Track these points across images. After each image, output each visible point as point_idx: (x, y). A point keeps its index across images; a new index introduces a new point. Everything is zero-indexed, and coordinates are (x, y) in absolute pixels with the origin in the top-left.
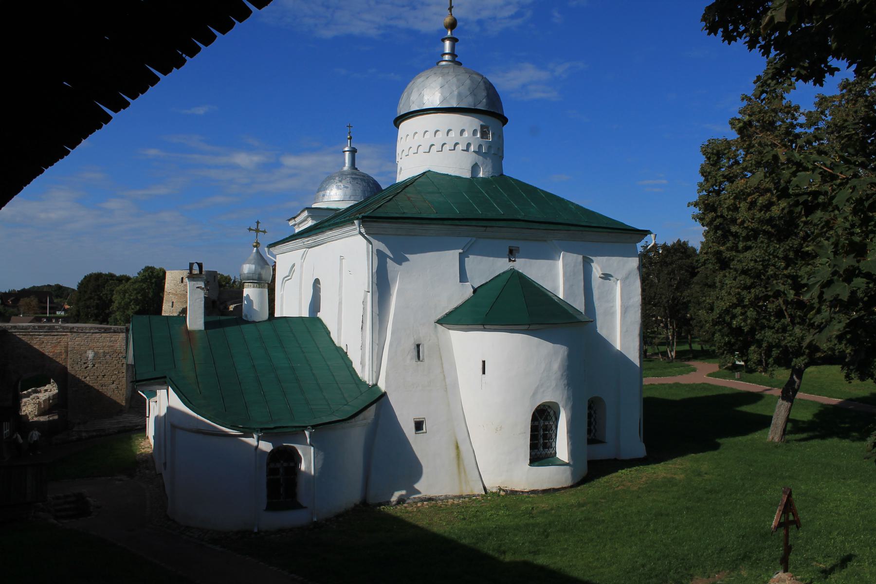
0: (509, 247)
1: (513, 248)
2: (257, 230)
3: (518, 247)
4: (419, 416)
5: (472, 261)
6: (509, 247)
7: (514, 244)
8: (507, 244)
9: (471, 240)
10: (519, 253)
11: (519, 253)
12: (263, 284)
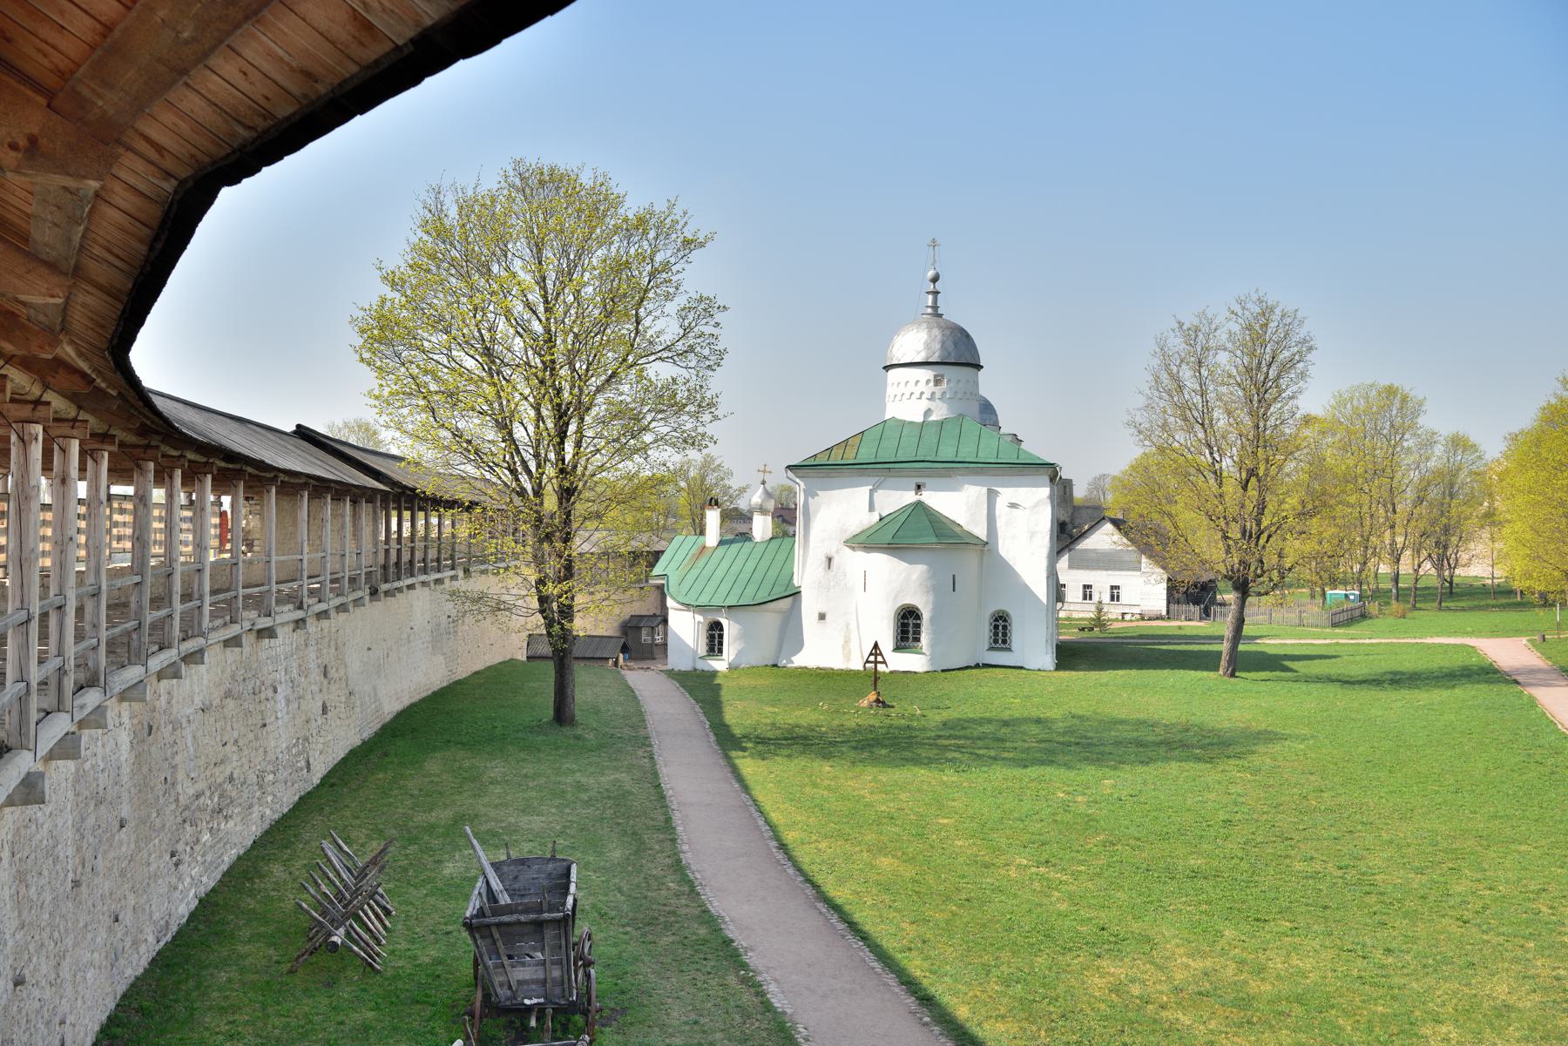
2: (764, 472)
4: (823, 611)
5: (880, 495)
8: (914, 481)
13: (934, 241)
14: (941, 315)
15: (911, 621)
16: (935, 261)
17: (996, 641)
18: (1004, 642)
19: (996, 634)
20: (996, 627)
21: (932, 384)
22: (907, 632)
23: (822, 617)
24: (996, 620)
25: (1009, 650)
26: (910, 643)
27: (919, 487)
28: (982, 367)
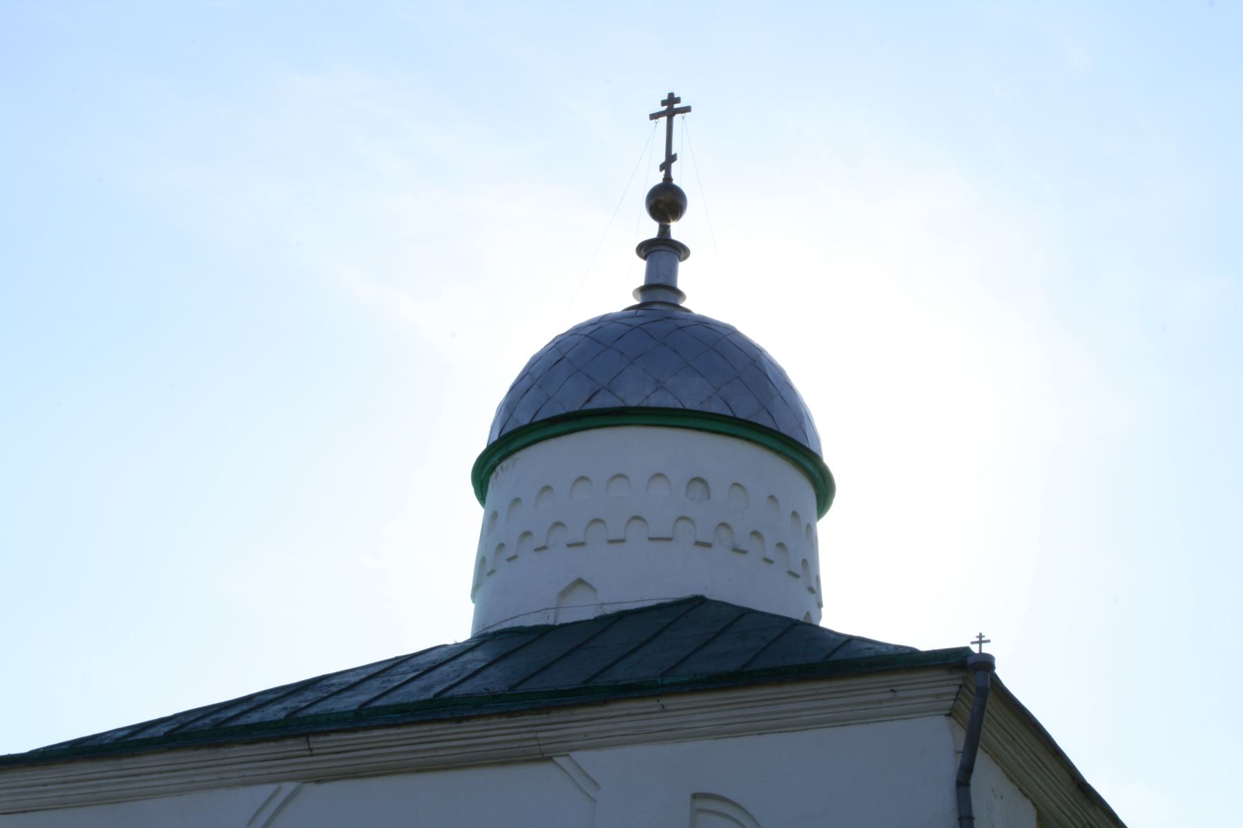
13: (671, 100)
16: (670, 158)
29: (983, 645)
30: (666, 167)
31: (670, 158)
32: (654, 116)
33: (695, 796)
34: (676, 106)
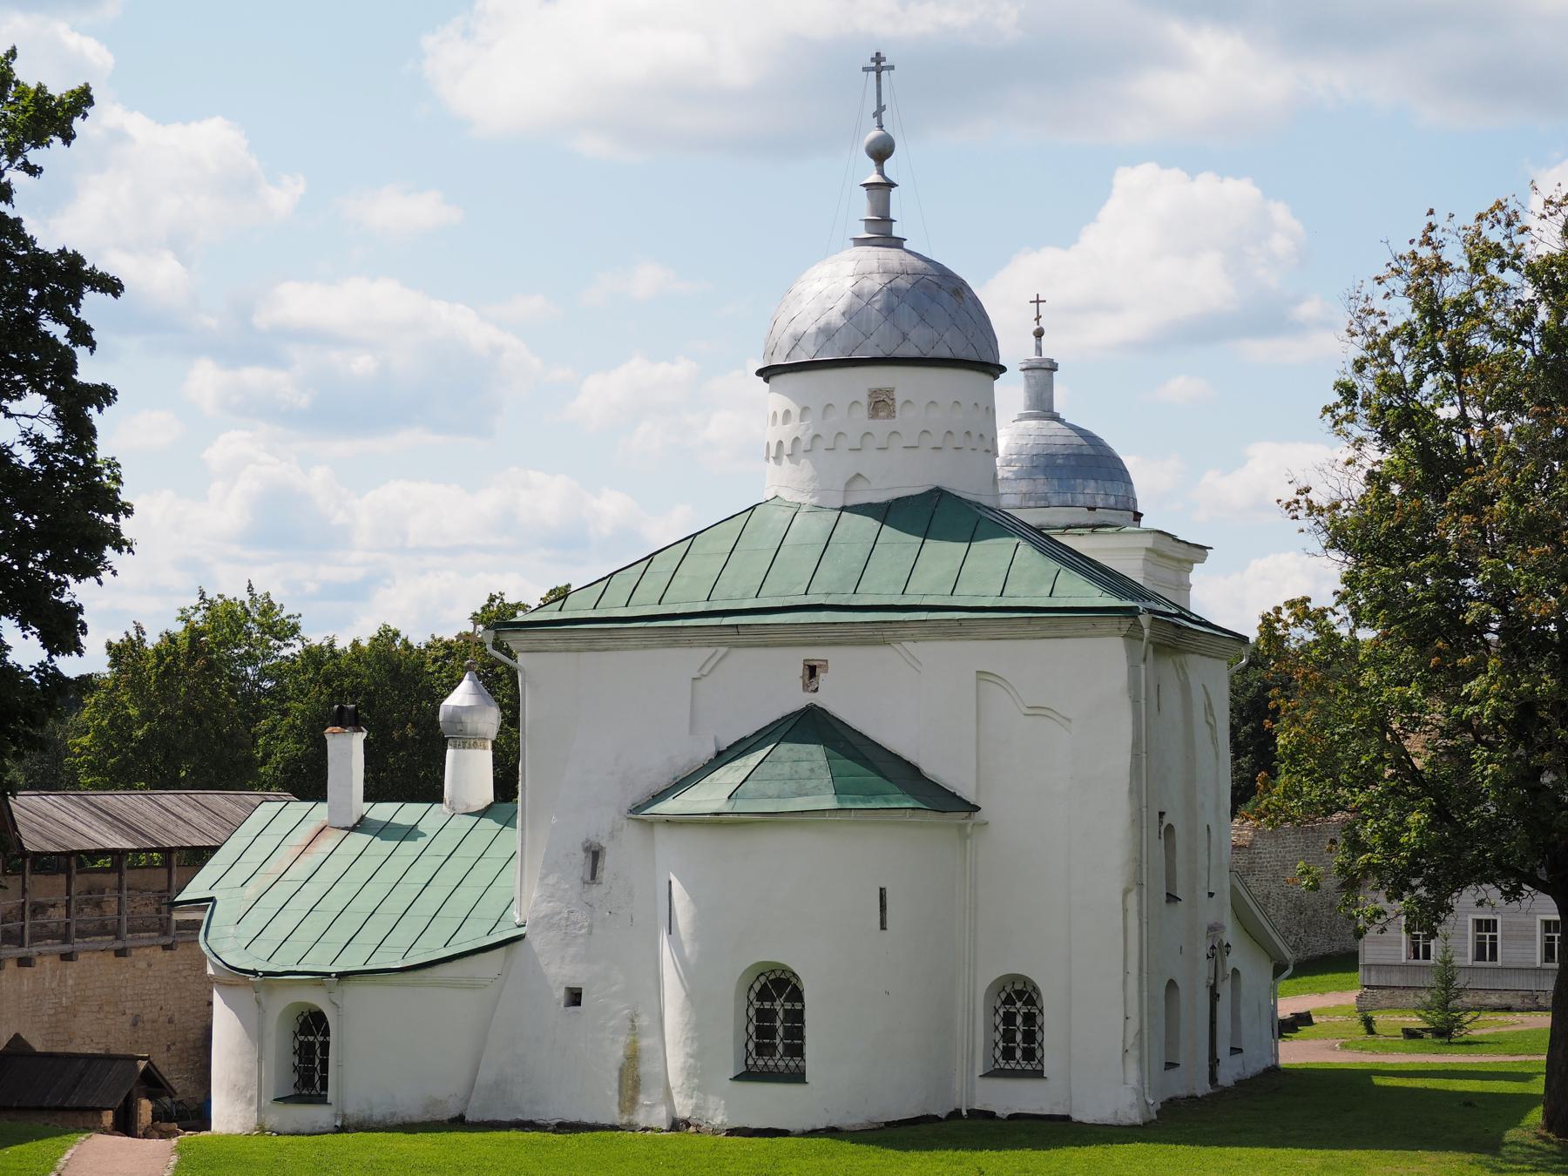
0: (804, 660)
1: (815, 663)
3: (826, 661)
6: (804, 660)
7: (815, 654)
8: (794, 660)
9: (715, 653)
10: (826, 672)
11: (826, 672)
12: (472, 742)
13: (878, 58)
14: (898, 243)
15: (781, 1006)
16: (881, 109)
17: (1008, 1054)
18: (1029, 1055)
19: (1008, 1036)
20: (1009, 1019)
21: (862, 412)
22: (772, 1033)
23: (575, 997)
24: (1009, 1001)
25: (1039, 1074)
26: (779, 1062)
27: (812, 671)
28: (1003, 369)
29: (1040, 304)
30: (878, 114)
31: (881, 109)
32: (865, 69)
33: (977, 672)
34: (883, 64)
